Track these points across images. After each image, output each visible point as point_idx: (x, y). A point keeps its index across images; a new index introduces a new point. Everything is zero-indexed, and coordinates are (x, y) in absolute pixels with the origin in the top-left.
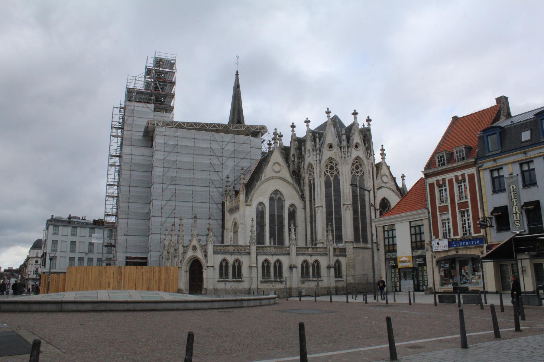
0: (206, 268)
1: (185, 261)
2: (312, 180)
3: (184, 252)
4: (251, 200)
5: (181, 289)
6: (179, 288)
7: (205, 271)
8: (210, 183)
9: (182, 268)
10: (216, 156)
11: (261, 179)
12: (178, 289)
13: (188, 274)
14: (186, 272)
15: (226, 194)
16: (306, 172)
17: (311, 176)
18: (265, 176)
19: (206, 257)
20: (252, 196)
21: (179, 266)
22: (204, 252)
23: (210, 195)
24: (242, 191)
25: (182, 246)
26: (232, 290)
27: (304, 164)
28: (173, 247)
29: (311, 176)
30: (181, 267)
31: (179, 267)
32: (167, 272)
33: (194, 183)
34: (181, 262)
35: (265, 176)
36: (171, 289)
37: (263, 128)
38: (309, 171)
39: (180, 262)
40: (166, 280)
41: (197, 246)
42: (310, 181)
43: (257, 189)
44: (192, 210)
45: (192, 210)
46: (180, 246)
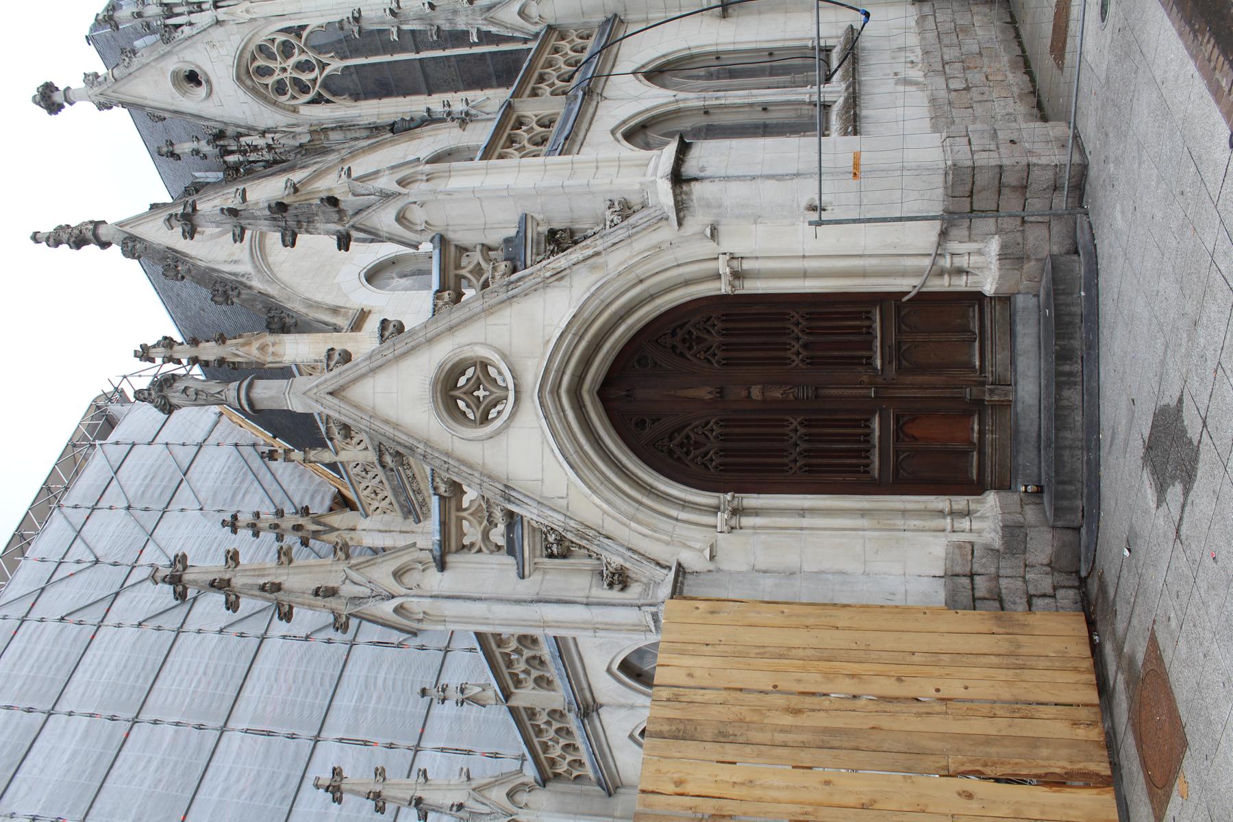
0: (697, 222)
1: (611, 527)
2: (323, 66)
3: (511, 551)
4: (335, 310)
5: (950, 576)
6: (941, 597)
7: (730, 244)
8: (242, 635)
9: (692, 560)
10: (117, 594)
11: (243, 276)
12: (952, 603)
13: (752, 501)
14: (736, 512)
15: (316, 534)
16: (291, 119)
17: (306, 77)
18: (236, 262)
19: (572, 233)
20: (317, 306)
21: (665, 590)
22: (514, 270)
23: (307, 638)
24: (262, 348)
25: (442, 566)
26: (929, 71)
27: (251, 129)
28: (522, 798)
29: (306, 77)
30: (681, 570)
31: (677, 592)
32: (722, 737)
33: (210, 724)
34: (620, 579)
35: (236, 262)
36: (953, 688)
37: (98, 408)
38: (283, 99)
39: (615, 595)
40: (828, 740)
41: (443, 352)
42: (333, 89)
43: (285, 286)
44: (366, 743)
45: (366, 743)
46: (434, 580)
